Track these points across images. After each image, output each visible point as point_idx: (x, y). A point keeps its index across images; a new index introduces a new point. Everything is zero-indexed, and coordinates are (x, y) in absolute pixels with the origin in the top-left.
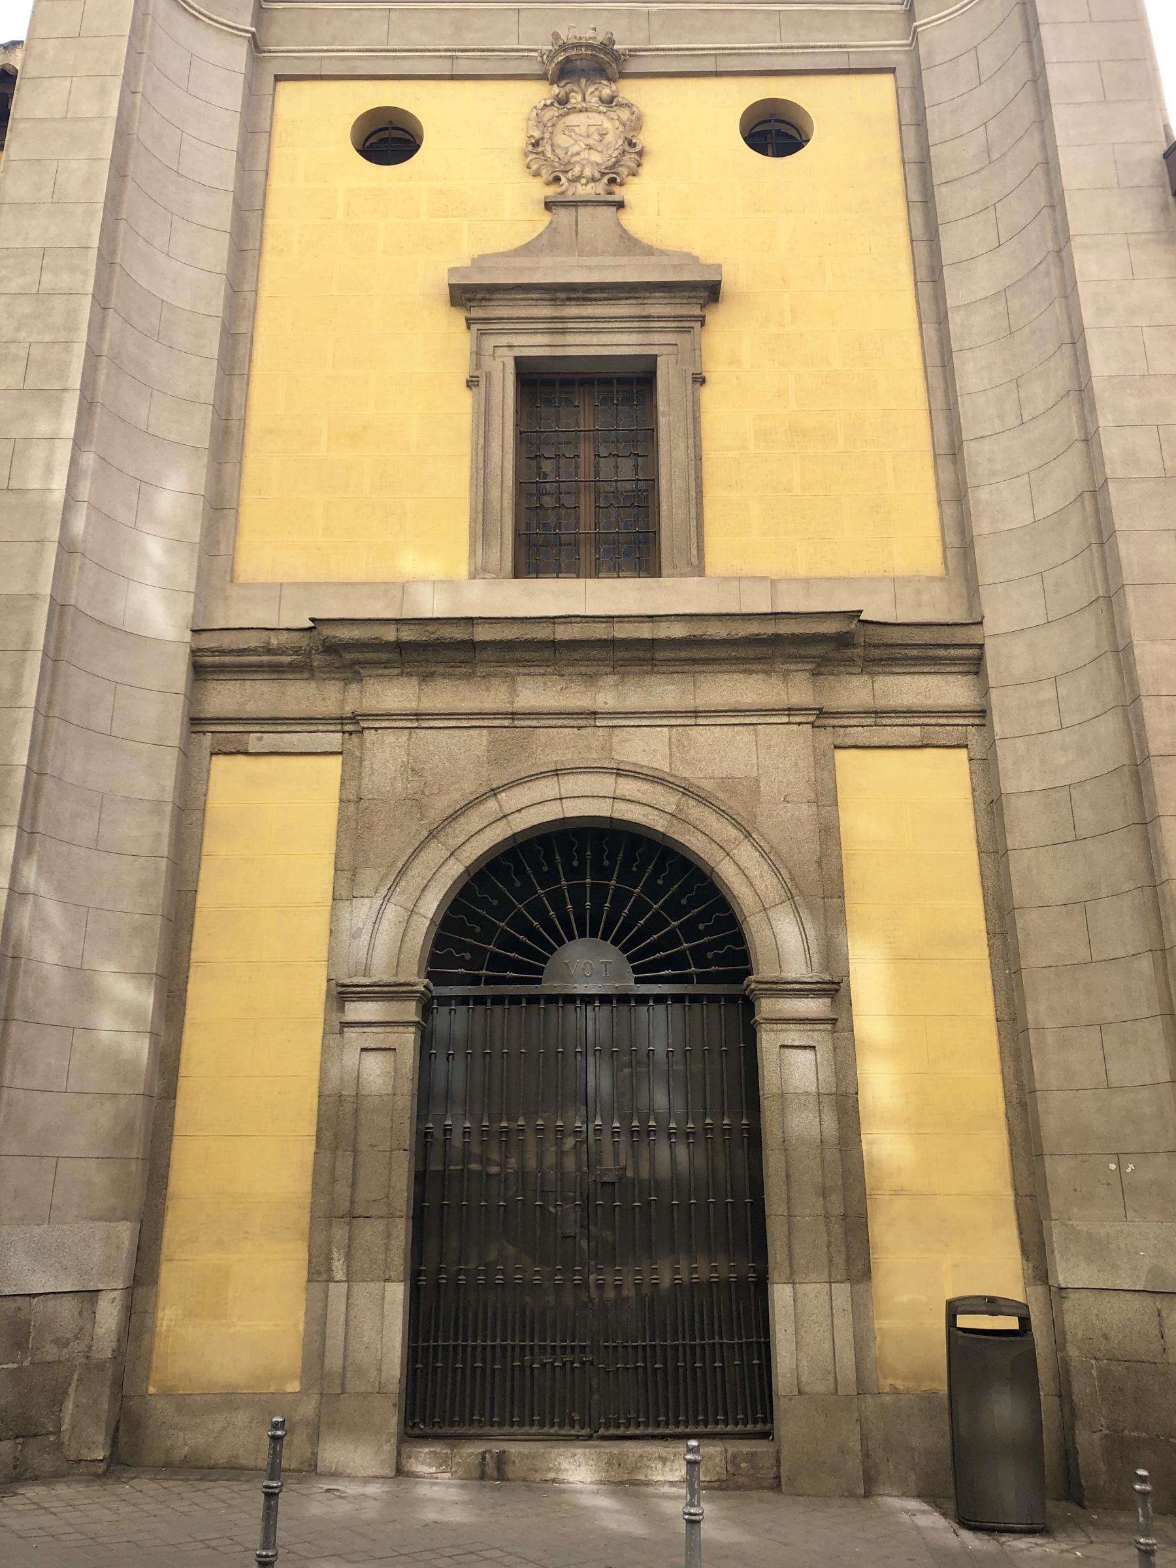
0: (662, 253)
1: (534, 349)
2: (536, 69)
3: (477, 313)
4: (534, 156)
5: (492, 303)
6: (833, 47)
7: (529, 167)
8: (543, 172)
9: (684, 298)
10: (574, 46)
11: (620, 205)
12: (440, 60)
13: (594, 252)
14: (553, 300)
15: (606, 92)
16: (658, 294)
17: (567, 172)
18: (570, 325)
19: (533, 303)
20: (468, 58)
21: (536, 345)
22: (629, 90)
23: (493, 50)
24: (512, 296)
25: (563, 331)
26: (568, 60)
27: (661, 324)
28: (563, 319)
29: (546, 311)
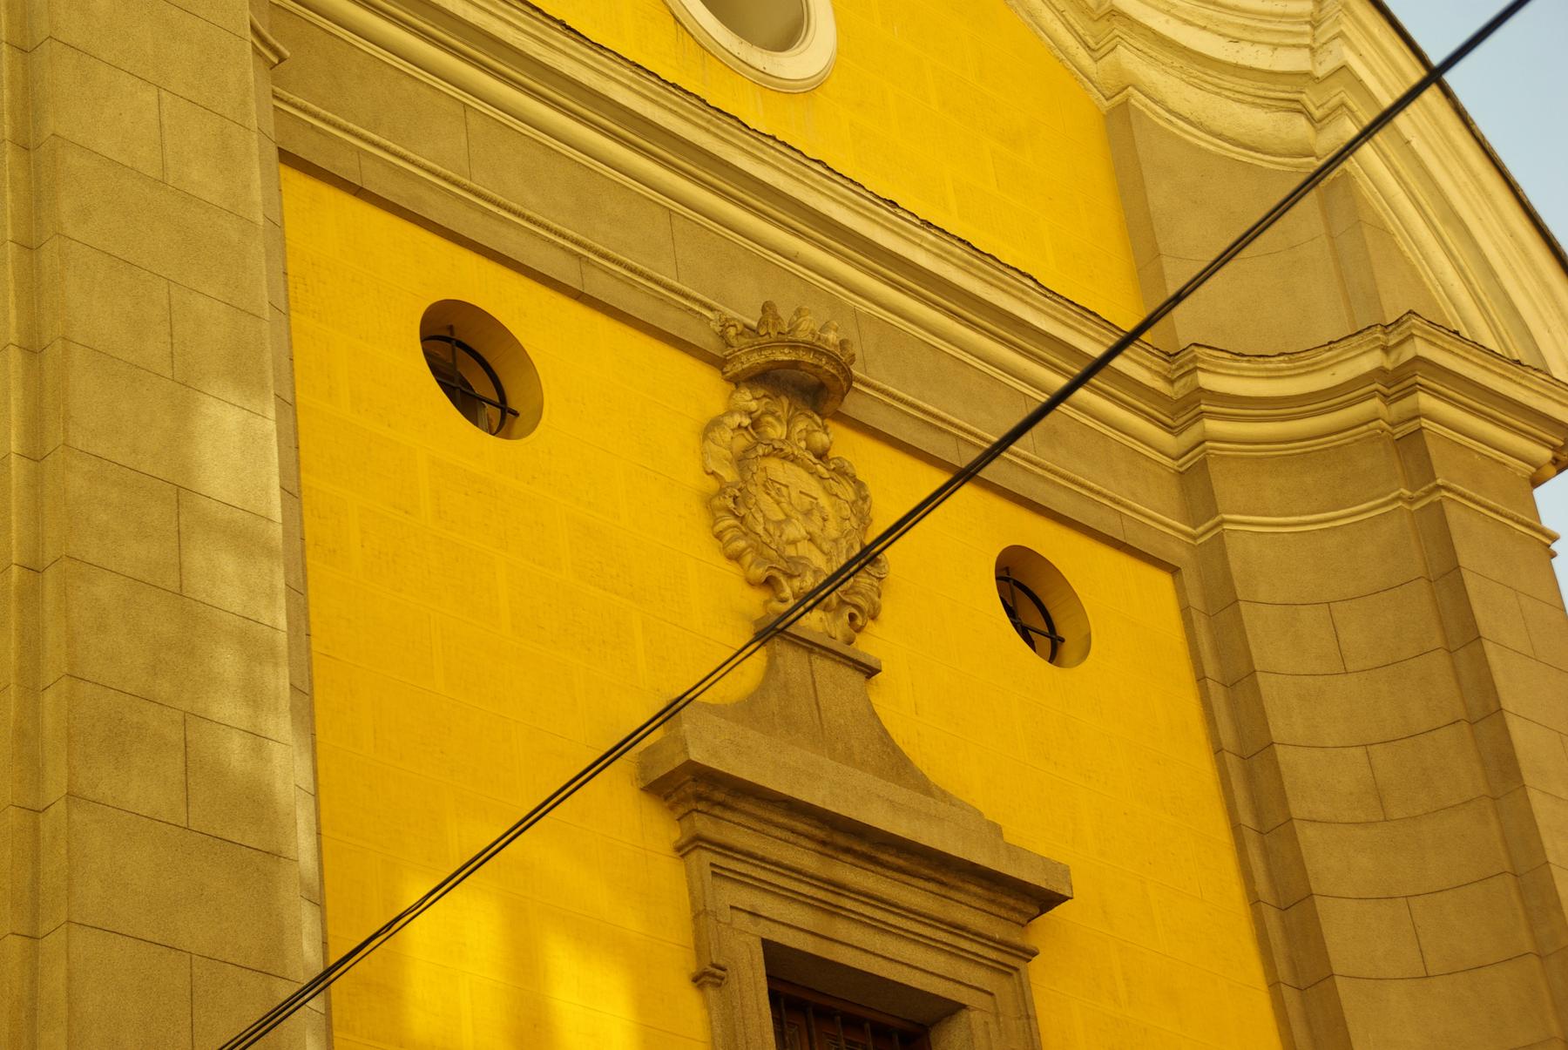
0: (945, 796)
1: (790, 932)
2: (711, 344)
3: (704, 825)
4: (733, 521)
5: (728, 815)
6: (1105, 496)
7: (719, 536)
8: (748, 559)
9: (1001, 905)
10: (811, 348)
11: (870, 671)
12: (560, 254)
13: (848, 758)
14: (823, 843)
15: (820, 439)
16: (973, 888)
17: (790, 576)
18: (849, 904)
19: (792, 837)
20: (607, 271)
21: (797, 926)
22: (847, 445)
23: (649, 278)
24: (767, 815)
25: (833, 911)
26: (795, 364)
27: (975, 948)
28: (839, 888)
29: (808, 861)
